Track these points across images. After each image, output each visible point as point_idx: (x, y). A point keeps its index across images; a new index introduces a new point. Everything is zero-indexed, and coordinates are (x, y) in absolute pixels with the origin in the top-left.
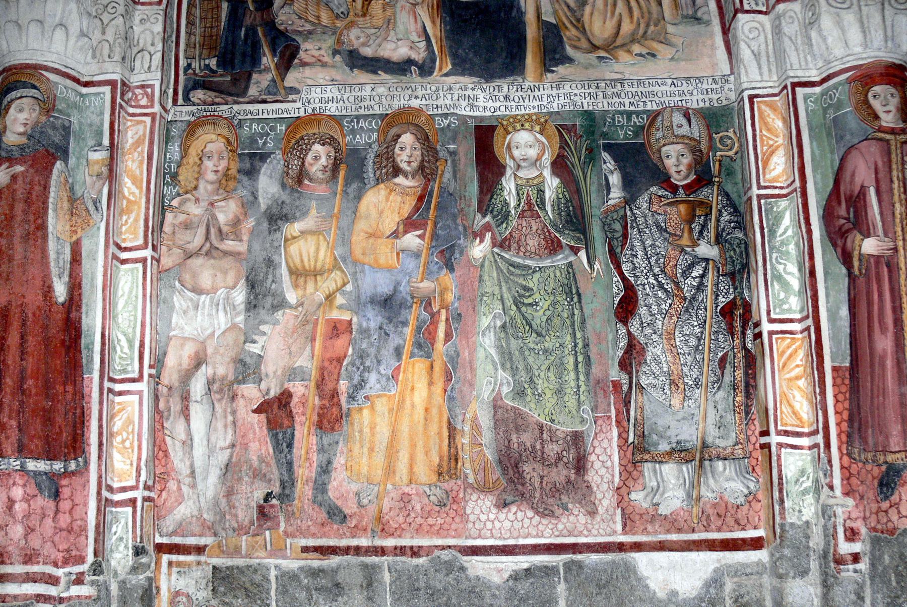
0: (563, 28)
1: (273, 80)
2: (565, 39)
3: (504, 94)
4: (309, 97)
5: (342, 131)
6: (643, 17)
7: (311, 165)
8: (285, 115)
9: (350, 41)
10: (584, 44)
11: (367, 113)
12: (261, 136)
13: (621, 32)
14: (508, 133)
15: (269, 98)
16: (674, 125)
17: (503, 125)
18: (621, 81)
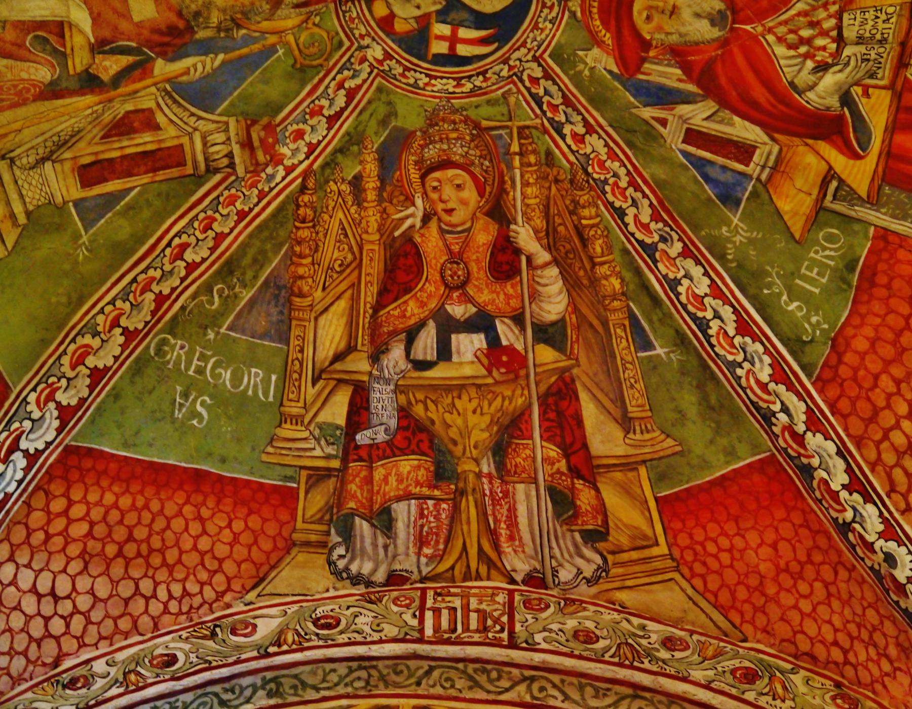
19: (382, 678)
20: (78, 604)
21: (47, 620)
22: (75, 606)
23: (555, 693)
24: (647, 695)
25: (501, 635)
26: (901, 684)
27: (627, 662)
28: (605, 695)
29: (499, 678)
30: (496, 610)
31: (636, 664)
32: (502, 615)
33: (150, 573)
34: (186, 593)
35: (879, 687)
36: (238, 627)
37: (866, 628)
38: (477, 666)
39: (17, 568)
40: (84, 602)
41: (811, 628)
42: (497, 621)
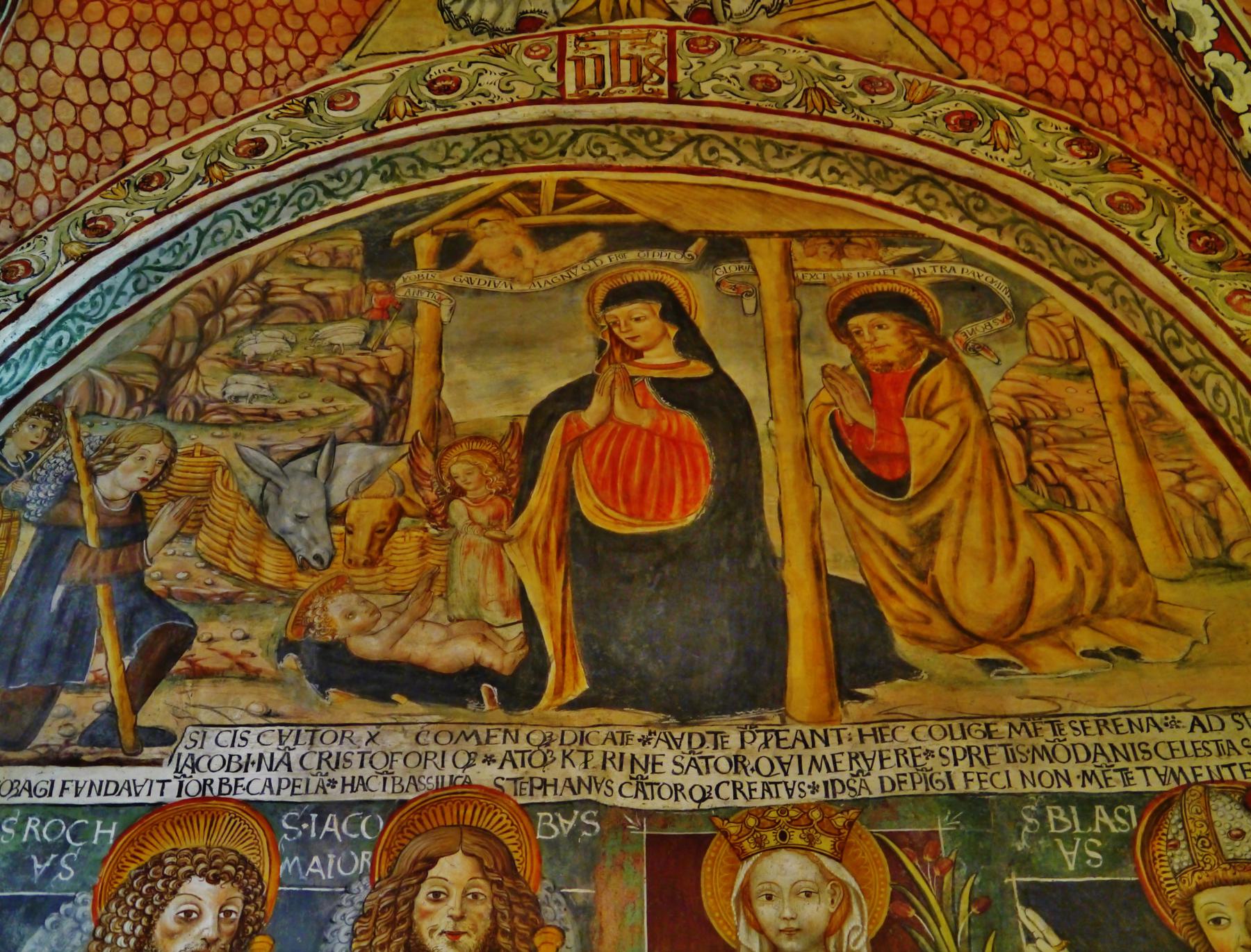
0: (882, 592)
1: (111, 711)
2: (890, 620)
3: (731, 753)
4: (198, 753)
5: (273, 843)
6: (1090, 567)
7: (171, 935)
8: (124, 798)
9: (328, 620)
10: (940, 628)
11: (349, 796)
12: (45, 850)
13: (1038, 602)
14: (743, 857)
15: (86, 753)
16: (1221, 832)
17: (726, 834)
18: (1054, 719)
19: (518, 148)
20: (135, 85)
21: (102, 108)
22: (132, 89)
23: (729, 154)
24: (841, 151)
25: (660, 87)
26: (1154, 123)
27: (815, 112)
28: (789, 154)
29: (660, 140)
30: (652, 55)
31: (826, 114)
32: (660, 61)
33: (219, 39)
34: (267, 61)
35: (1125, 127)
36: (337, 98)
37: (1114, 54)
38: (632, 127)
39: (52, 47)
40: (143, 83)
41: (1046, 57)
42: (655, 68)
